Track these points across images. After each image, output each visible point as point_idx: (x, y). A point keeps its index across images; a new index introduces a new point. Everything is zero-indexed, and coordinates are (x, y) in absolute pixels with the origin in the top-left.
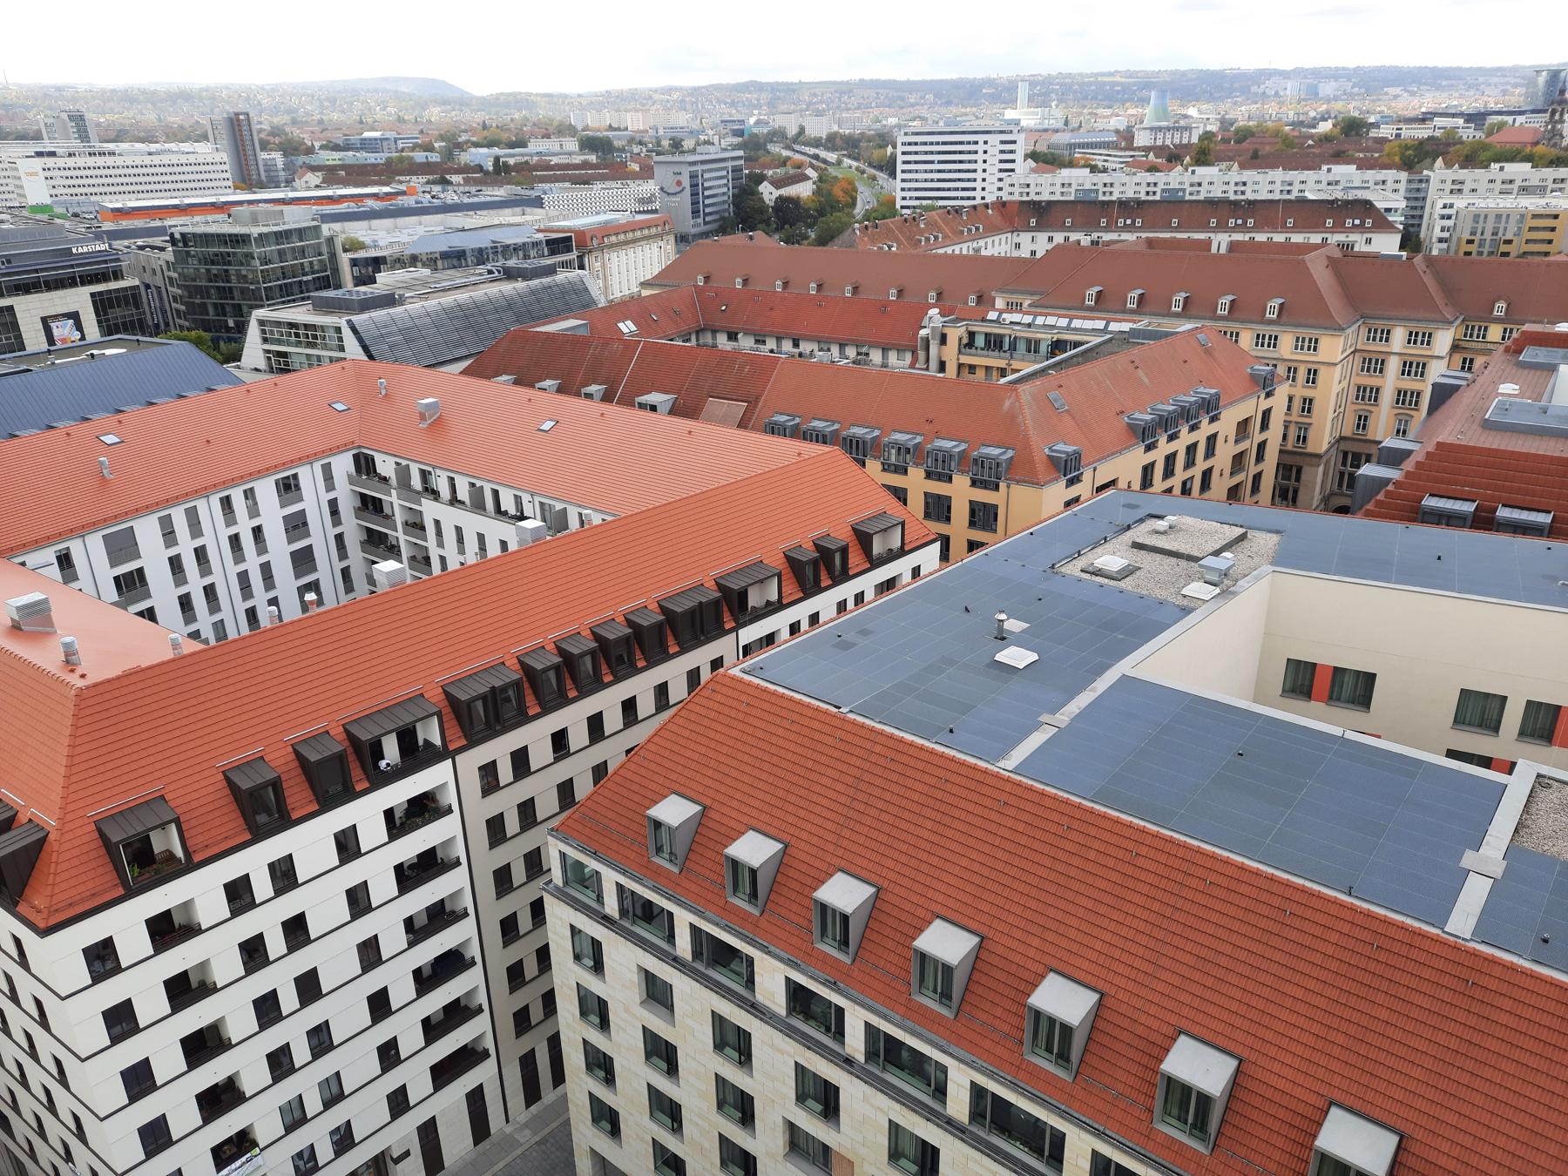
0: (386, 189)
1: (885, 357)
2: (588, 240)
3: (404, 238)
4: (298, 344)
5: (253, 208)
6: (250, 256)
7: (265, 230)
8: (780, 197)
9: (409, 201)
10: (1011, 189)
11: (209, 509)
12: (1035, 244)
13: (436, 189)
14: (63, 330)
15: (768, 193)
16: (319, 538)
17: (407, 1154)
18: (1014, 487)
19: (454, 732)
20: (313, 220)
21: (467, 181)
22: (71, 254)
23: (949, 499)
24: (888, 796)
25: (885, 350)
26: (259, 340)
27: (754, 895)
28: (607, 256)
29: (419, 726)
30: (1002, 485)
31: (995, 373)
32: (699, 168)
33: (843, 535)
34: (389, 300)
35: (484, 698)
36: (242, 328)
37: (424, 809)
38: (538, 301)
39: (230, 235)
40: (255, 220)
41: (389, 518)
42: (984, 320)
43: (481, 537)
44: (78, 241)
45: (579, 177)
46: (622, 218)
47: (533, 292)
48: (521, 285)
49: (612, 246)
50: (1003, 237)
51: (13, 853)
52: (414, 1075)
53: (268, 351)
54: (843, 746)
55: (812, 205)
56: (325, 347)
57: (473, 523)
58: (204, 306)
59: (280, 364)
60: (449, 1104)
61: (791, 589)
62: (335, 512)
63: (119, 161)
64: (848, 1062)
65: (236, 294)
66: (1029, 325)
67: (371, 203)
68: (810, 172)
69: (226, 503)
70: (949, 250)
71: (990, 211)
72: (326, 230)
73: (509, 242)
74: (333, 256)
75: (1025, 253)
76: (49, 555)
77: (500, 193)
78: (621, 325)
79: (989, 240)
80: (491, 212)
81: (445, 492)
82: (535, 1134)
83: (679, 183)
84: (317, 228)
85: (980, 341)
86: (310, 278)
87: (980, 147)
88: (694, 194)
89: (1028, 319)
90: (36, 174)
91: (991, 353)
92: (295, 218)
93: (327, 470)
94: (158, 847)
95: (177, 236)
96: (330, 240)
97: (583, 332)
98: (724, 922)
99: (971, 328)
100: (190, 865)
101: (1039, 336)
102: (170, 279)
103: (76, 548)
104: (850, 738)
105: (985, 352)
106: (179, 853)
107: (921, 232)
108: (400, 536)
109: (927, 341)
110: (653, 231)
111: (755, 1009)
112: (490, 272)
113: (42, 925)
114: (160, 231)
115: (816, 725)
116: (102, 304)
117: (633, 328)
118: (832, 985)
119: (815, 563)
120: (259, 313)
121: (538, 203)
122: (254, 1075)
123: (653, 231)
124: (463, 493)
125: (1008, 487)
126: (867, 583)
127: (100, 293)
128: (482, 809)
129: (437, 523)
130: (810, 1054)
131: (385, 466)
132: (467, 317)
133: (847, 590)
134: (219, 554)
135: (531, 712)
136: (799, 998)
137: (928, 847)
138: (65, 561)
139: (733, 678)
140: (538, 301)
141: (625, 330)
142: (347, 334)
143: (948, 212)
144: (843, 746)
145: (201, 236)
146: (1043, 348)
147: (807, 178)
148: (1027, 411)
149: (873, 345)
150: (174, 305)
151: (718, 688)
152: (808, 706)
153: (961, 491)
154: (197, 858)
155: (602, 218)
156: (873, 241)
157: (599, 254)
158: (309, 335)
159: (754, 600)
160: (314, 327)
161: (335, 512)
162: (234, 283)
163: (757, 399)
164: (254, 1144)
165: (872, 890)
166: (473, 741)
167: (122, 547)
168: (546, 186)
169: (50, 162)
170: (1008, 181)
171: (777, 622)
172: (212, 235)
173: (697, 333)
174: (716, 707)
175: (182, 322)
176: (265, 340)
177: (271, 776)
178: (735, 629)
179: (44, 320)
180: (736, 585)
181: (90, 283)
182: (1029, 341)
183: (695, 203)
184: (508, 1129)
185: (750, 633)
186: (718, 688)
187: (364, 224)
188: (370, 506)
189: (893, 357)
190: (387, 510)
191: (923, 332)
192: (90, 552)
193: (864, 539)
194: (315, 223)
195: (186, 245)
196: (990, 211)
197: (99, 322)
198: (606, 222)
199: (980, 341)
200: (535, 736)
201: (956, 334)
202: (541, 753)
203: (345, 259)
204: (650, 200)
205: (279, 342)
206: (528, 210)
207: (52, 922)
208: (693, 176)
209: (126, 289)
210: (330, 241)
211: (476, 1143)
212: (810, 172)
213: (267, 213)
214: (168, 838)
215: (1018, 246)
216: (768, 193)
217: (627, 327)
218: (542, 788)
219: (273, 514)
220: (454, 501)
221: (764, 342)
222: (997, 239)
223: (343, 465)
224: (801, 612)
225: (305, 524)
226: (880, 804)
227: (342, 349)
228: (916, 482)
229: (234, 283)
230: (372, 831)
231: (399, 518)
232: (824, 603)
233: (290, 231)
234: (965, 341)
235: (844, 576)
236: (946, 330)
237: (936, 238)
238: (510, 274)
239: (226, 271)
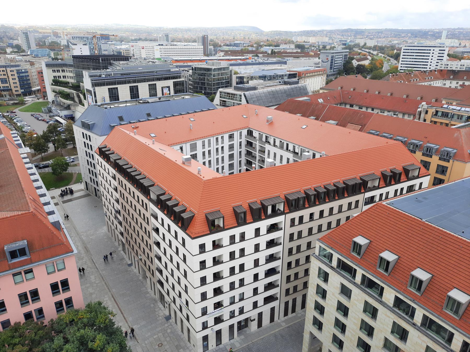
0: (243, 58)
1: (403, 116)
2: (301, 74)
3: (248, 72)
4: (229, 99)
5: (213, 61)
6: (211, 74)
7: (216, 67)
8: (359, 65)
9: (250, 61)
10: (441, 66)
11: (213, 140)
12: (453, 84)
13: (256, 58)
14: (166, 91)
15: (355, 63)
16: (236, 152)
17: (254, 320)
18: (456, 163)
19: (286, 208)
21: (264, 56)
23: (430, 163)
24: (439, 249)
25: (404, 114)
26: (219, 97)
27: (386, 270)
28: (306, 79)
29: (277, 205)
30: (451, 161)
31: (444, 125)
32: (334, 55)
33: (399, 169)
34: (254, 88)
35: (295, 200)
36: (215, 93)
37: (273, 228)
38: (293, 91)
40: (213, 65)
41: (254, 148)
42: (442, 107)
43: (281, 157)
44: (172, 68)
45: (296, 56)
46: (312, 69)
47: (292, 89)
48: (289, 86)
49: (308, 77)
50: (440, 81)
51: (188, 218)
52: (260, 299)
54: (423, 231)
55: (369, 68)
56: (236, 100)
57: (279, 152)
58: (197, 87)
59: (223, 104)
60: (266, 309)
61: (382, 183)
62: (240, 145)
63: (177, 47)
64: (414, 325)
65: (206, 84)
66: (459, 110)
67: (239, 61)
68: (369, 57)
69: (217, 139)
70: (423, 84)
71: (436, 73)
72: (231, 68)
73: (279, 74)
74: (231, 75)
75: (447, 86)
76: (178, 147)
77: (274, 60)
78: (319, 100)
79: (435, 82)
80: (272, 65)
81: (272, 142)
82: (286, 324)
83: (327, 59)
84: (228, 67)
85: (440, 114)
86: (224, 81)
87: (431, 52)
88: (332, 62)
89: (459, 108)
90: (158, 50)
91: (443, 118)
92: (224, 64)
93: (241, 133)
94: (216, 223)
95: (194, 68)
96: (231, 71)
97: (308, 101)
98: (374, 275)
99: (437, 110)
100: (223, 229)
101: (463, 114)
102: (190, 79)
103: (184, 146)
104: (426, 229)
105: (442, 118)
106: (222, 225)
107: (412, 78)
108: (257, 154)
109: (420, 113)
110: (321, 73)
111: (381, 303)
112: (280, 82)
113: (193, 237)
114: (190, 66)
115: (413, 223)
116: (175, 84)
117: (322, 101)
118: (413, 301)
119: (391, 177)
120: (221, 90)
121: (285, 63)
122: (226, 288)
123: (321, 73)
124: (278, 143)
125: (453, 162)
126: (405, 185)
127: (175, 82)
128: (289, 230)
129: (269, 151)
130: (399, 319)
131: (256, 134)
132: (274, 94)
133: (399, 187)
134: (213, 152)
135: (306, 206)
136: (398, 302)
137: (453, 266)
138: (181, 148)
139: (384, 205)
140: (293, 91)
141: (320, 101)
142: (243, 97)
143: (422, 72)
144: (423, 231)
145: (199, 68)
146: (464, 119)
147: (368, 59)
148: (463, 138)
149: (400, 112)
150: (189, 86)
151: (378, 207)
152: (411, 217)
153: (435, 161)
154: (226, 228)
155: (306, 68)
156: (395, 79)
157: (304, 79)
158: (232, 96)
159: (370, 185)
160: (234, 95)
161: (240, 145)
162: (206, 81)
163: (365, 125)
164: (222, 306)
165: (431, 276)
166: (291, 212)
167: (194, 147)
168: (288, 58)
169: (161, 47)
170: (441, 63)
171: (376, 193)
172: (202, 68)
173: (340, 104)
174: (377, 213)
175: (190, 91)
176: (221, 97)
177: (244, 210)
178: (364, 193)
179: (162, 88)
180: (366, 179)
181: (173, 79)
182: (459, 115)
183: (331, 65)
184: (279, 321)
185: (369, 195)
186: (378, 207)
187: (238, 67)
188: (249, 144)
189: (406, 117)
190: (254, 146)
191: (419, 110)
192: (187, 147)
193: (406, 171)
195: (195, 70)
196: (436, 73)
197: (174, 89)
198: (307, 70)
199: (440, 114)
200: (306, 213)
201: (432, 111)
202: (306, 219)
203: (234, 77)
204: (318, 64)
205: (224, 98)
206: (283, 65)
207: (195, 236)
208: (332, 57)
211: (270, 322)
212: (369, 57)
213: (217, 63)
214: (219, 221)
215: (445, 84)
216: (355, 63)
217: (321, 101)
218: (304, 228)
219: (227, 143)
220: (275, 145)
221: (362, 108)
222: (437, 82)
223: (245, 132)
224: (383, 191)
225: (233, 147)
226: (436, 250)
227: (241, 101)
228: (419, 155)
229: (206, 81)
230: (263, 231)
231: (258, 148)
232: (391, 189)
234: (434, 113)
235: (398, 182)
236: (428, 110)
237: (417, 80)
238: (285, 83)
239: (204, 78)
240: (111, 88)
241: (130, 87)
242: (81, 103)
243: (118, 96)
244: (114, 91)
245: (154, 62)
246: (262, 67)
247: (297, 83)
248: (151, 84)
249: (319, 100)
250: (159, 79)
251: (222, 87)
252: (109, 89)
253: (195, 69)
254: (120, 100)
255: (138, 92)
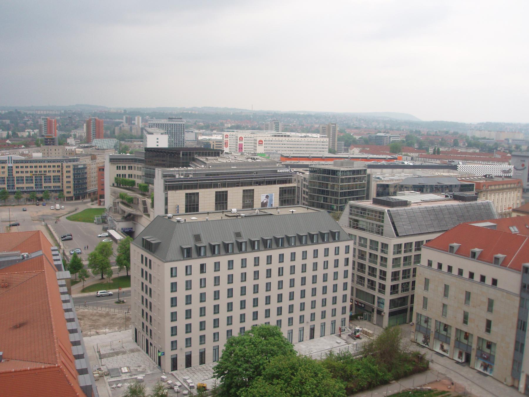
4: (363, 217)
5: (342, 160)
7: (346, 169)
20: (365, 167)
22: (277, 172)
28: (489, 195)
34: (405, 203)
36: (342, 209)
38: (468, 211)
39: (332, 170)
40: (342, 165)
44: (280, 167)
47: (466, 207)
53: (351, 219)
63: (290, 139)
72: (369, 171)
74: (369, 182)
78: (511, 228)
80: (434, 170)
83: (523, 165)
84: (365, 170)
92: (358, 166)
96: (369, 176)
110: (513, 186)
114: (306, 166)
116: (283, 191)
117: (517, 230)
121: (455, 168)
123: (513, 186)
127: (283, 188)
141: (513, 230)
142: (387, 216)
150: (303, 195)
157: (485, 193)
176: (351, 214)
194: (365, 168)
197: (280, 198)
204: (509, 171)
205: (356, 215)
209: (291, 187)
210: (369, 176)
217: (514, 230)
233: (361, 170)
238: (456, 198)
239: (327, 184)
240: (190, 194)
241: (216, 192)
242: (146, 210)
243: (198, 205)
244: (193, 198)
245: (254, 159)
246: (419, 172)
247: (475, 199)
248: (247, 190)
249: (511, 228)
250: (259, 183)
251: (353, 199)
252: (187, 194)
253: (313, 171)
254: (201, 210)
255: (227, 200)
